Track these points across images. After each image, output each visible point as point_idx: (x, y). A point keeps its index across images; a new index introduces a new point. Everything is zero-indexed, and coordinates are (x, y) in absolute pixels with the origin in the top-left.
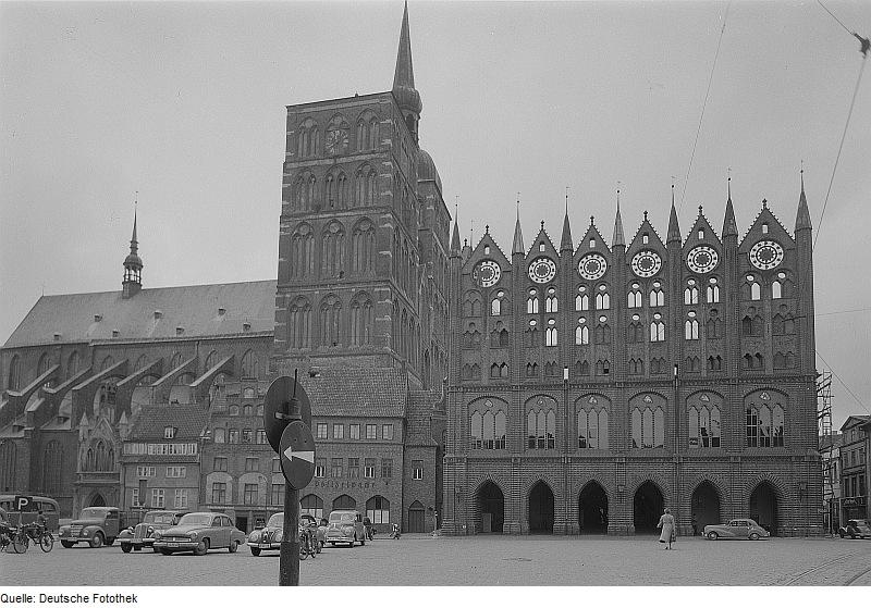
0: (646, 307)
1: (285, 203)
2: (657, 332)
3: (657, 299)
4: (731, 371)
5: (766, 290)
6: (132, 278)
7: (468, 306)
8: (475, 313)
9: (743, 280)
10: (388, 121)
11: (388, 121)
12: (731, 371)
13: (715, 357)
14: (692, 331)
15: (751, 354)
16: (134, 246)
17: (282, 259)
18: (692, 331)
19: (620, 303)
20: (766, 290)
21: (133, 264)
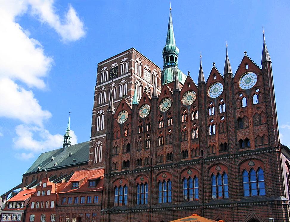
2: (196, 134)
7: (116, 133)
11: (131, 60)
12: (232, 149)
13: (223, 143)
14: (212, 130)
15: (242, 139)
17: (93, 126)
18: (212, 130)
19: (178, 121)
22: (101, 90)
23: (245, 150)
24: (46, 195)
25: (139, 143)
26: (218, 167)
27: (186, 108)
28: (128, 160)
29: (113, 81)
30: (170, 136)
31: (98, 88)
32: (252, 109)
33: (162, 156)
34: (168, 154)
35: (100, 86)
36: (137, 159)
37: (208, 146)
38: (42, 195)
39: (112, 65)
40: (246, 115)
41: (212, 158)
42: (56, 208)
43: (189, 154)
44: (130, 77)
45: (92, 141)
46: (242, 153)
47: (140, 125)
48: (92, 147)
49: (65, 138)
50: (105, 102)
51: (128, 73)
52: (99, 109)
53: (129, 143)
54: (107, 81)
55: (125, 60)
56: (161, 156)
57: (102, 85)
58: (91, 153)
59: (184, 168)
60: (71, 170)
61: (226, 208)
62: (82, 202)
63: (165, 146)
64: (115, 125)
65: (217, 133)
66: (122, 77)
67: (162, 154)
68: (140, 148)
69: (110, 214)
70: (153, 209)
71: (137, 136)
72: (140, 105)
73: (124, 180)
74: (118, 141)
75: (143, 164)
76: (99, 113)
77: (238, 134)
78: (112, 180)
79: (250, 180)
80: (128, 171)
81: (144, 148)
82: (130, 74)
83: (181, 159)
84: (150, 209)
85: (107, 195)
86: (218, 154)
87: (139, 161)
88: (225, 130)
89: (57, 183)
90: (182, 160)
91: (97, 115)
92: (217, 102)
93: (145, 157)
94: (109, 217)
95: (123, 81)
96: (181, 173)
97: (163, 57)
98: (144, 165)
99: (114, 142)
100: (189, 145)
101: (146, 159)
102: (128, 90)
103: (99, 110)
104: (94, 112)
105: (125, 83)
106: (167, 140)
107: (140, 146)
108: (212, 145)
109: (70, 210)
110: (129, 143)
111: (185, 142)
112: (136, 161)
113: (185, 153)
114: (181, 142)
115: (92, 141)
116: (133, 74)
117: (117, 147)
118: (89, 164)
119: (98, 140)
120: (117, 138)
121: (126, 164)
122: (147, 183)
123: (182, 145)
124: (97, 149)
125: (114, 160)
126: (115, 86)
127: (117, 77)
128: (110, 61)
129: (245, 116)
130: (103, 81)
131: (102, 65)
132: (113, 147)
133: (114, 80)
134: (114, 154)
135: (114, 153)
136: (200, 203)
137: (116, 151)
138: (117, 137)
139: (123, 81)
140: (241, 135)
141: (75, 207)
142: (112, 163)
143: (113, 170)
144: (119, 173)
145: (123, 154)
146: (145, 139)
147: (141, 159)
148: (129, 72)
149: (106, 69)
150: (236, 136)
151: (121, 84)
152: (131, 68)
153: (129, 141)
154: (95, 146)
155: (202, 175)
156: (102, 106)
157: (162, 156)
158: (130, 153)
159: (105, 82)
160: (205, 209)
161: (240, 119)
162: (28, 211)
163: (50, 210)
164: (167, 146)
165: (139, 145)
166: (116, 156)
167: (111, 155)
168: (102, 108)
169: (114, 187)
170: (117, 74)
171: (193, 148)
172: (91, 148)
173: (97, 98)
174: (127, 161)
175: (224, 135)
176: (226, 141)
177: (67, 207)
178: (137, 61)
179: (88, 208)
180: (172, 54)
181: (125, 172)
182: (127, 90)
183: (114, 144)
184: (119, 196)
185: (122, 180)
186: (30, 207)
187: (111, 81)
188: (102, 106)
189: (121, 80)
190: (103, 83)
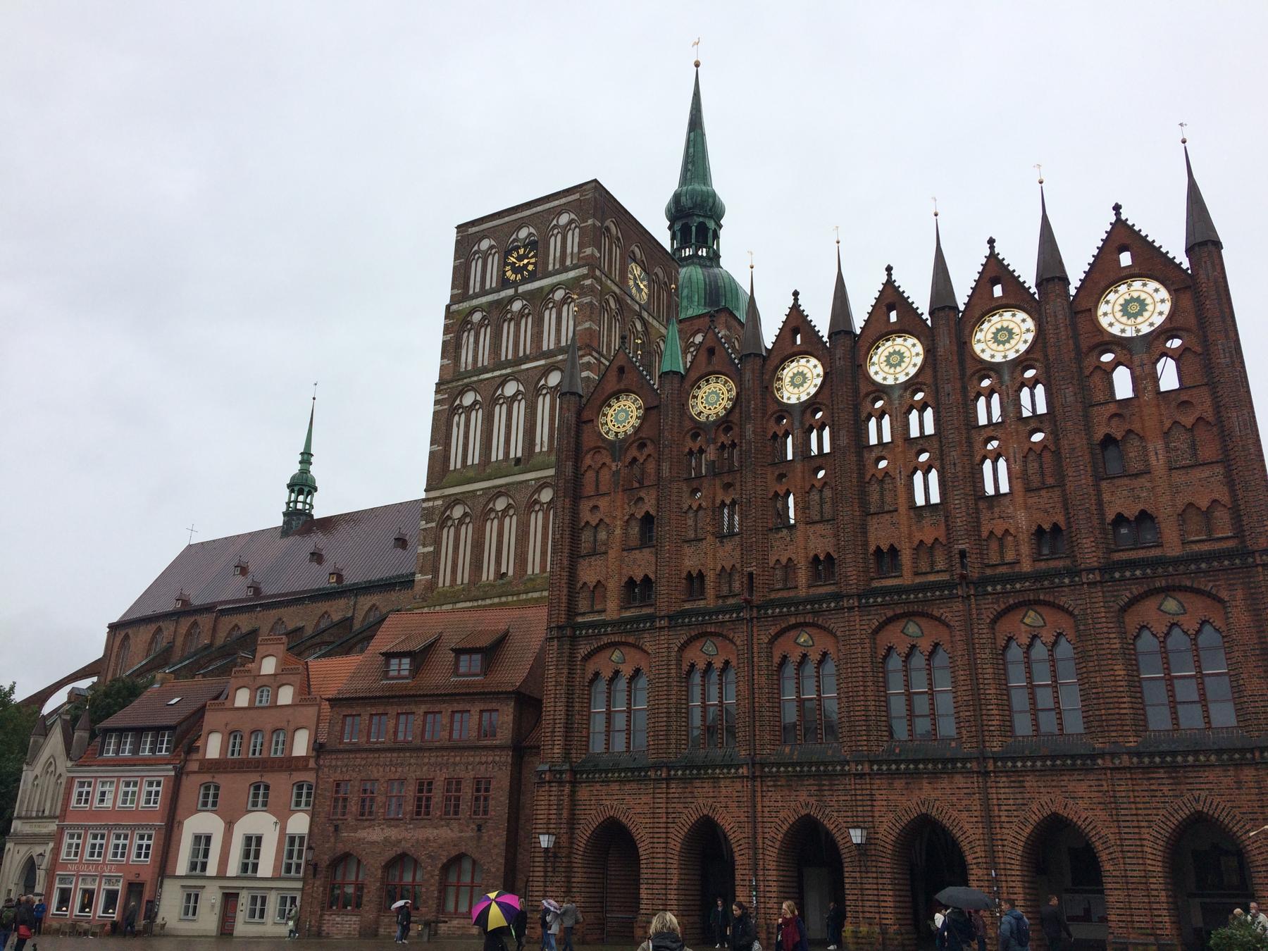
0: (905, 443)
1: (446, 362)
3: (923, 423)
4: (1089, 551)
5: (1145, 380)
6: (300, 506)
8: (603, 489)
9: (1089, 362)
10: (590, 222)
11: (590, 222)
13: (1046, 527)
16: (306, 457)
17: (435, 448)
20: (1145, 380)
21: (302, 485)
22: (470, 322)
23: (1133, 555)
24: (274, 706)
25: (691, 514)
26: (911, 623)
27: (886, 393)
28: (646, 576)
29: (516, 291)
30: (821, 491)
31: (458, 312)
32: (1158, 406)
33: (790, 566)
34: (816, 557)
35: (465, 305)
36: (684, 575)
37: (985, 534)
38: (257, 704)
39: (514, 236)
40: (1136, 427)
41: (1004, 579)
42: (318, 757)
43: (906, 558)
44: (588, 282)
45: (431, 504)
46: (1132, 564)
47: (695, 449)
48: (429, 525)
49: (292, 491)
50: (486, 363)
51: (575, 267)
52: (461, 388)
53: (647, 513)
54: (492, 291)
55: (564, 219)
56: (786, 566)
57: (475, 302)
58: (424, 547)
59: (890, 614)
60: (320, 613)
61: (1082, 770)
62: (427, 737)
63: (801, 527)
64: (588, 440)
65: (1019, 486)
66: (555, 281)
67: (790, 559)
68: (696, 531)
69: (574, 783)
70: (763, 765)
71: (685, 488)
72: (694, 375)
73: (632, 650)
74: (603, 503)
75: (710, 592)
76: (461, 401)
77: (1106, 497)
78: (583, 650)
79: (1055, 676)
80: (651, 618)
81: (713, 534)
82: (584, 271)
83: (873, 579)
84: (754, 764)
85: (561, 707)
86: (1026, 566)
87: (695, 582)
88: (1050, 481)
89: (317, 657)
90: (875, 584)
91: (454, 411)
92: (1013, 379)
93: (719, 567)
94: (573, 793)
95: (559, 295)
96: (877, 631)
97: (670, 228)
98: (718, 597)
99: (585, 506)
100: (904, 530)
101: (725, 574)
103: (462, 393)
104: (440, 397)
105: (564, 301)
106: (808, 508)
107: (696, 525)
108: (999, 533)
109: (377, 764)
110: (647, 513)
111: (887, 516)
112: (684, 581)
113: (887, 557)
114: (869, 517)
115: (431, 504)
116: (598, 273)
117: (598, 525)
118: (418, 589)
119: (499, 495)
120: (599, 495)
121: (639, 590)
122: (734, 662)
123: (873, 524)
124: (448, 536)
125: (589, 573)
126: (527, 311)
127: (533, 277)
128: (507, 219)
129: (1130, 431)
130: (477, 290)
131: (473, 230)
132: (583, 524)
133: (521, 289)
134: (584, 552)
135: (585, 546)
136: (967, 749)
137: (595, 540)
138: (597, 486)
139: (559, 295)
140: (1120, 501)
141: (402, 755)
142: (579, 585)
143: (583, 614)
144: (613, 624)
145: (625, 553)
146: (718, 502)
147: (701, 576)
148: (581, 263)
149: (491, 247)
150: (1100, 503)
151: (551, 305)
152: (588, 251)
153: (649, 506)
154: (442, 525)
155: (970, 643)
156: (475, 379)
157: (790, 566)
158: (653, 549)
159: (484, 293)
160: (994, 772)
161: (1109, 440)
162: (194, 766)
163: (291, 764)
164: (811, 529)
165: (690, 522)
166: (597, 562)
167: (575, 556)
168: (514, 377)
169: (590, 676)
170: (535, 266)
171: (991, 532)
172: (425, 530)
173: (451, 349)
174: (641, 581)
175: (1046, 499)
176: (1060, 519)
177: (364, 755)
178: (608, 229)
179: (458, 758)
181: (637, 620)
183: (586, 515)
184: (609, 715)
185: (626, 650)
186: (201, 751)
187: (511, 292)
188: (475, 379)
189: (553, 289)
190: (476, 296)
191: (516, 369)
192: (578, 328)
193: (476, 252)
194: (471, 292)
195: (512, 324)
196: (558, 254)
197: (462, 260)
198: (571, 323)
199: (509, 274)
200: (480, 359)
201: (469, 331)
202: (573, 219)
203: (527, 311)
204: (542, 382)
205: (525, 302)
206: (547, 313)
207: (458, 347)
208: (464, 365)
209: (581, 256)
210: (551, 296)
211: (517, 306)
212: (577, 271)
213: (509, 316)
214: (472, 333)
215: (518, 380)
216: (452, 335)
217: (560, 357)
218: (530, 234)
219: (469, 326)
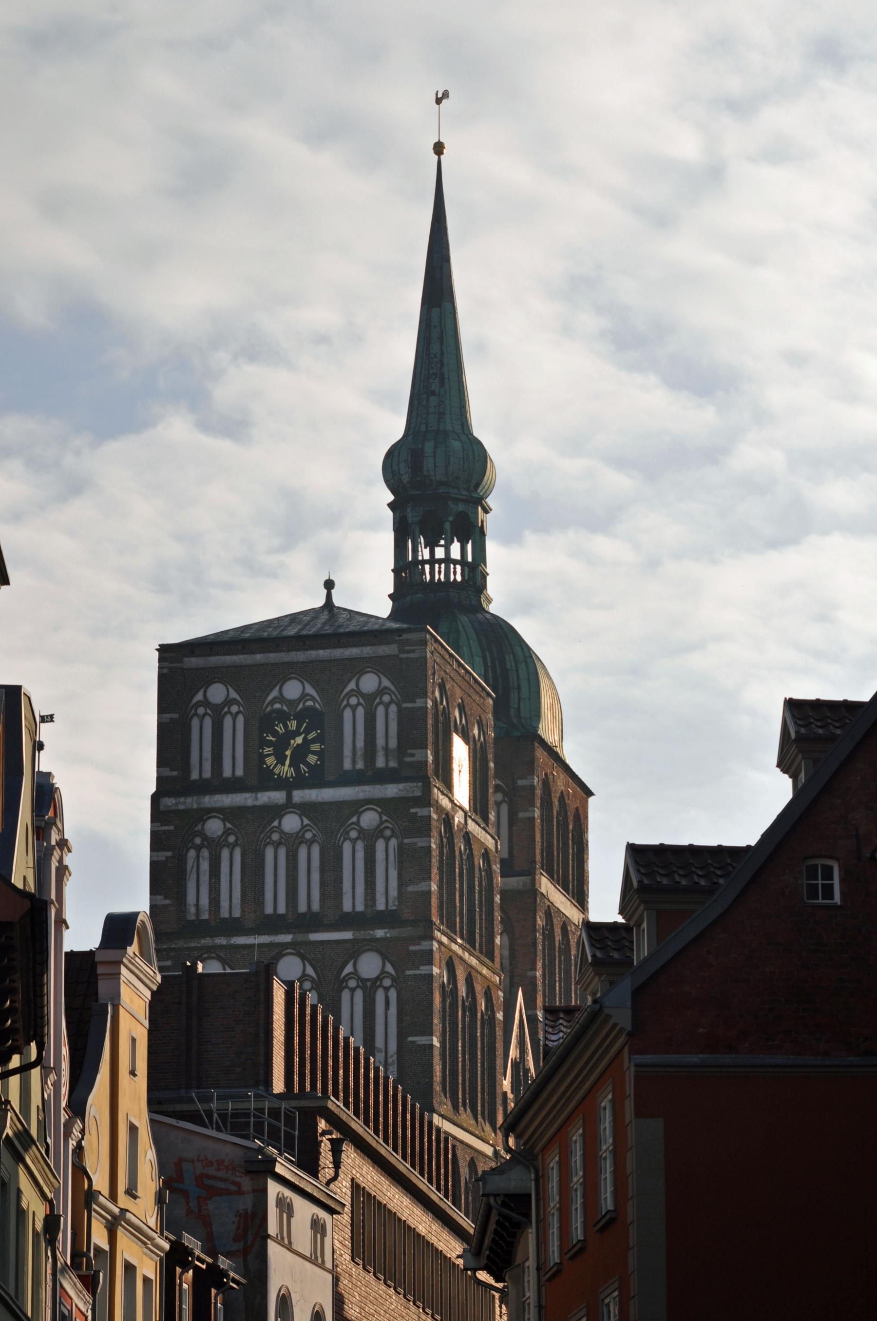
29: (289, 797)
44: (421, 812)
66: (361, 796)
95: (369, 819)
102: (410, 889)
127: (317, 779)
133: (299, 796)
152: (418, 755)
180: (461, 507)
182: (402, 884)
187: (277, 797)
189: (357, 806)
191: (300, 937)
192: (410, 889)
193: (198, 704)
194: (195, 776)
195: (282, 852)
196: (360, 744)
197: (175, 716)
198: (393, 874)
199: (270, 761)
200: (224, 903)
201: (198, 849)
202: (386, 688)
203: (309, 835)
204: (349, 969)
205: (306, 821)
206: (347, 847)
207: (181, 877)
208: (193, 910)
209: (407, 759)
210: (354, 819)
211: (291, 823)
212: (401, 786)
213: (275, 837)
214: (205, 853)
215: (303, 958)
216: (169, 854)
217: (380, 933)
218: (304, 696)
219: (198, 841)
